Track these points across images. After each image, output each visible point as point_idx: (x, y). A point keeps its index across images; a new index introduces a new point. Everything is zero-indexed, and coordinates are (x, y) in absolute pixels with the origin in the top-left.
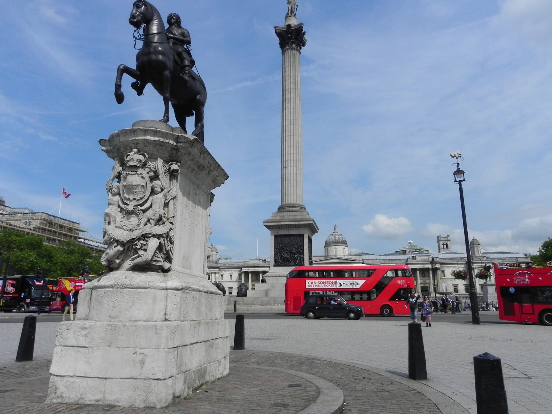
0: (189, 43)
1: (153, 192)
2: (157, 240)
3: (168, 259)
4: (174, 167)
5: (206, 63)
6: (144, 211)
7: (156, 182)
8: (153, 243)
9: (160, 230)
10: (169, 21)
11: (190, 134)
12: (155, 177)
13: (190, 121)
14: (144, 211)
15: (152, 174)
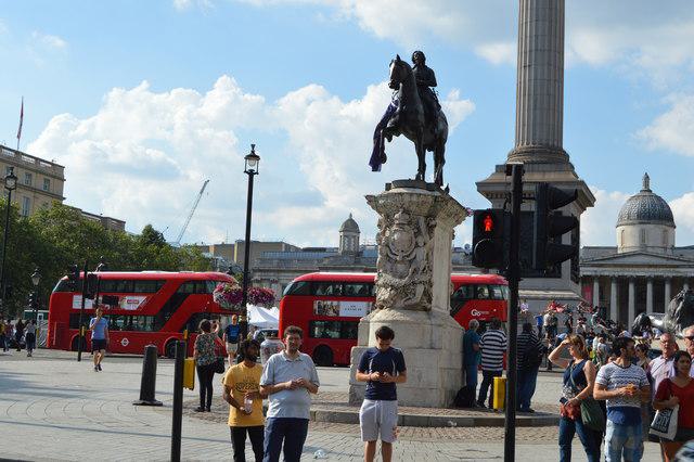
0: (436, 85)
1: (417, 246)
2: (423, 287)
3: (430, 301)
4: (433, 223)
5: (452, 103)
6: (411, 262)
7: (420, 240)
8: (420, 289)
9: (425, 278)
10: (414, 60)
11: (430, 177)
12: (418, 233)
13: (429, 156)
14: (411, 262)
15: (416, 231)
